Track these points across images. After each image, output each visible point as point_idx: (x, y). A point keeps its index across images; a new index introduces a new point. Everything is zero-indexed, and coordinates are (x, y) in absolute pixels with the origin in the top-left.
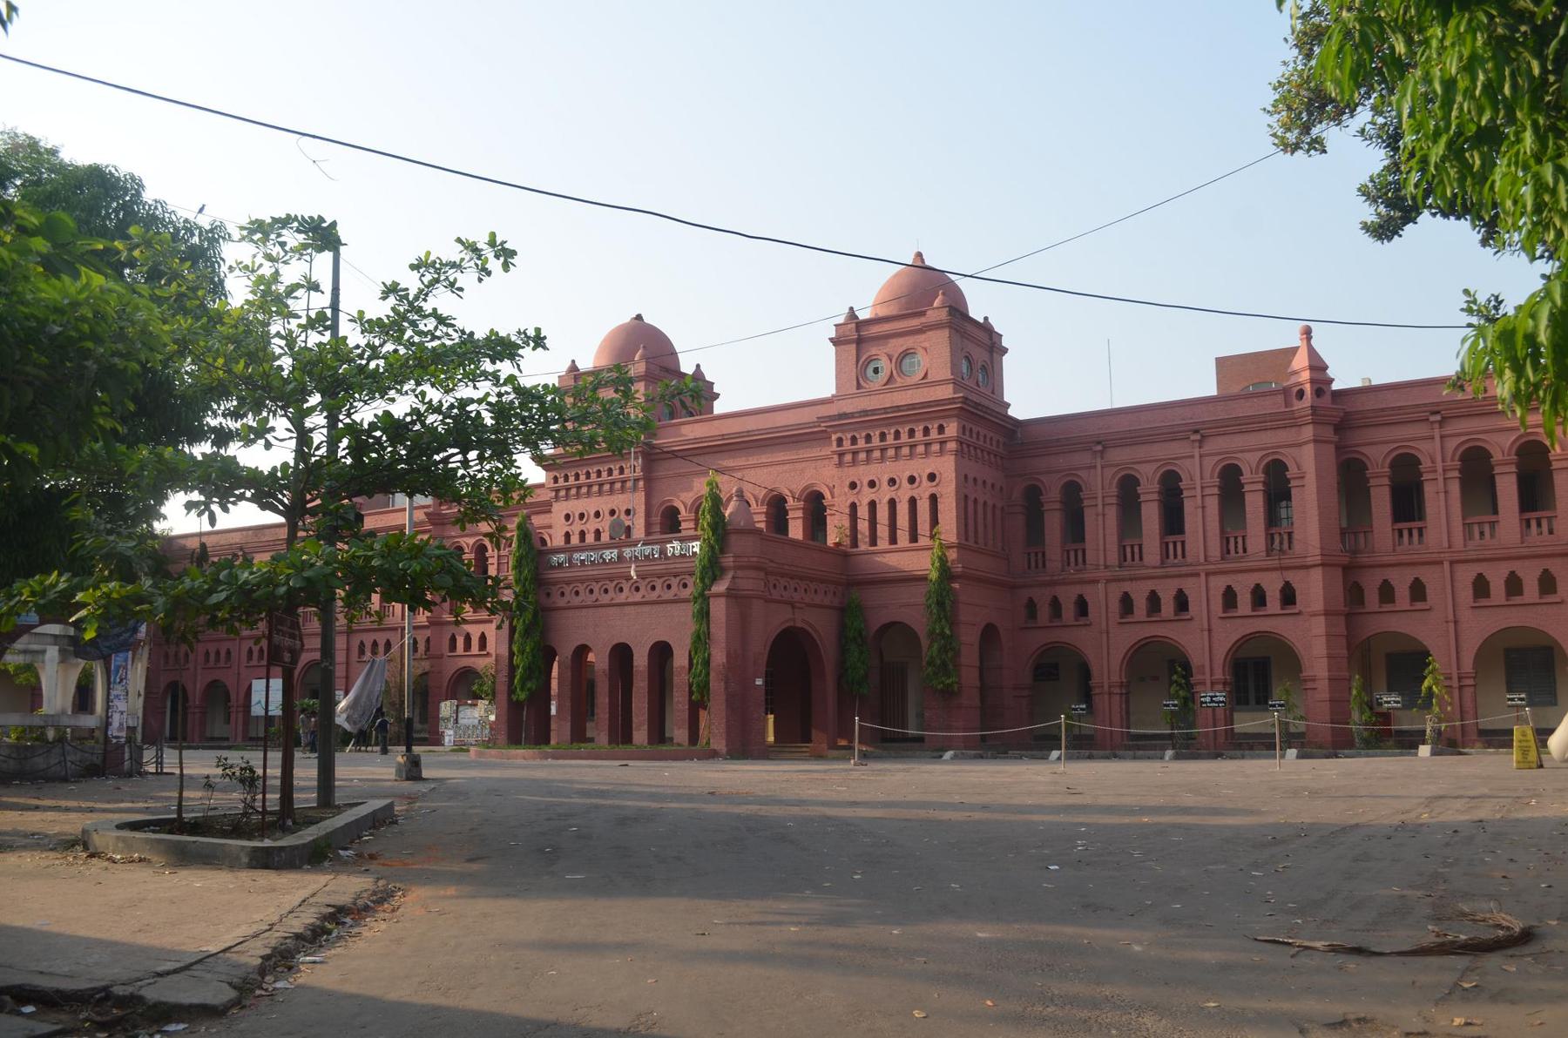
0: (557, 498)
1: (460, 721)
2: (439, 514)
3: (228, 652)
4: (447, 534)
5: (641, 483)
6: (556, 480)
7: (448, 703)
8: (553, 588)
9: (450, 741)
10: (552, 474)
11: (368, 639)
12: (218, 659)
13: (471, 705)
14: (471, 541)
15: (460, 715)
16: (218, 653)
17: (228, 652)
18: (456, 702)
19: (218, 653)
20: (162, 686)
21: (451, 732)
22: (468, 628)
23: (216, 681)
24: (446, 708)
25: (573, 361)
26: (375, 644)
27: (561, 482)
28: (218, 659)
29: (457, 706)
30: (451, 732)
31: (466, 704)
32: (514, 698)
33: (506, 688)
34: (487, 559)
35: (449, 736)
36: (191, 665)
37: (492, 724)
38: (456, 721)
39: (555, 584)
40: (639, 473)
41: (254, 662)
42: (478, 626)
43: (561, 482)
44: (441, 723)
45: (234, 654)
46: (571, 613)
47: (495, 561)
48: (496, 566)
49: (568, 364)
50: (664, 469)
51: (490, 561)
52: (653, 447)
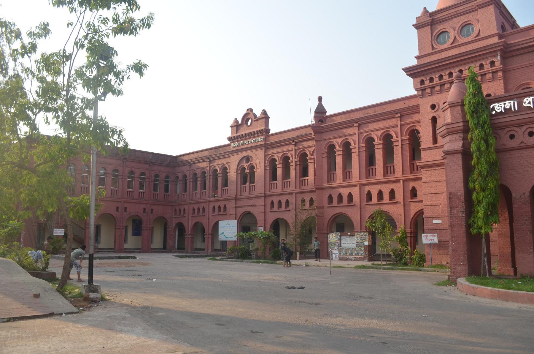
0: (423, 96)
1: (343, 245)
2: (319, 127)
3: (204, 208)
4: (324, 138)
5: (500, 74)
6: (422, 82)
7: (334, 234)
8: (499, 132)
9: (336, 257)
10: (419, 80)
11: (276, 200)
12: (199, 212)
13: (350, 235)
14: (340, 140)
15: (342, 242)
16: (199, 209)
17: (204, 208)
18: (339, 234)
19: (199, 209)
20: (174, 225)
21: (337, 252)
22: (341, 190)
23: (198, 222)
24: (333, 237)
25: (425, 8)
26: (280, 202)
27: (427, 83)
28: (199, 212)
29: (340, 236)
30: (337, 252)
31: (347, 235)
32: (475, 232)
33: (464, 223)
34: (351, 150)
35: (335, 253)
36: (186, 215)
37: (365, 247)
38: (340, 245)
39: (503, 128)
40: (498, 64)
41: (216, 213)
42: (346, 189)
43: (427, 83)
44: (330, 246)
45: (206, 209)
46: (525, 152)
47: (357, 150)
48: (357, 153)
49: (422, 10)
50: (516, 62)
51: (353, 150)
52: (508, 44)
